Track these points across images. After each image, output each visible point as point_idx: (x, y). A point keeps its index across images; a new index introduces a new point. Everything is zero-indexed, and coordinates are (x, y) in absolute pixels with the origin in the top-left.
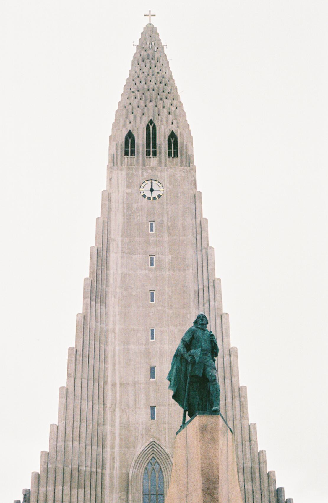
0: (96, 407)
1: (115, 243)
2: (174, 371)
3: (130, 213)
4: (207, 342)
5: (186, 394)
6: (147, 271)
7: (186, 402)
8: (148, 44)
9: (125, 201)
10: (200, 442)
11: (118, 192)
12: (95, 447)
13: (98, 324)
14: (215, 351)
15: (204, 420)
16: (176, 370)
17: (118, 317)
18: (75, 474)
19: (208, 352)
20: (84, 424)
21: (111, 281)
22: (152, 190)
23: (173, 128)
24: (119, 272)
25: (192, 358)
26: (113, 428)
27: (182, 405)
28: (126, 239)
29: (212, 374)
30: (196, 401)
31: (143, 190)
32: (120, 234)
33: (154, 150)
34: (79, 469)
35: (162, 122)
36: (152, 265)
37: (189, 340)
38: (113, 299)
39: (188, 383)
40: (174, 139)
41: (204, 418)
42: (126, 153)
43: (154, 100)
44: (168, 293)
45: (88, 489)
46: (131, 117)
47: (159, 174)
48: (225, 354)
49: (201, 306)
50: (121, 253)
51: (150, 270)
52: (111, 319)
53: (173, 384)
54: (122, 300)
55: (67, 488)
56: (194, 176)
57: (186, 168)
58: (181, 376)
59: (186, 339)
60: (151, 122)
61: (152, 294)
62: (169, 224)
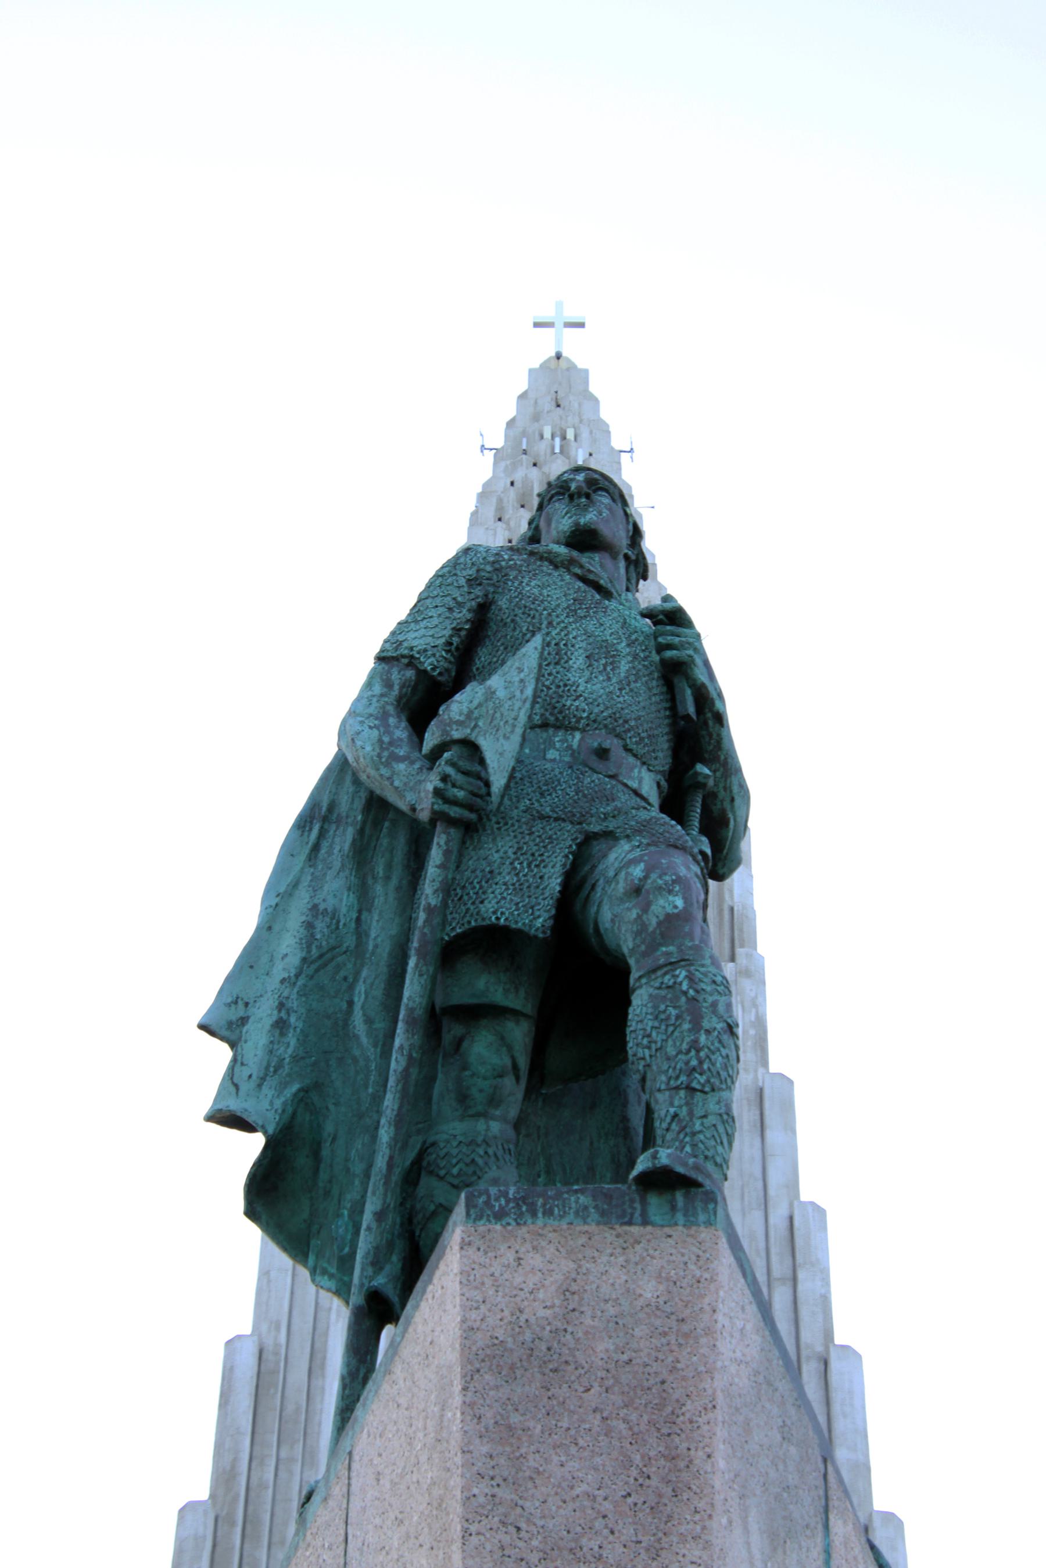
4: (624, 666)
7: (379, 1216)
8: (547, 435)
10: (466, 1534)
14: (702, 769)
15: (533, 1280)
16: (309, 939)
19: (627, 749)
39: (411, 1011)
41: (535, 1260)
56: (755, 1005)
58: (351, 1003)
59: (415, 643)
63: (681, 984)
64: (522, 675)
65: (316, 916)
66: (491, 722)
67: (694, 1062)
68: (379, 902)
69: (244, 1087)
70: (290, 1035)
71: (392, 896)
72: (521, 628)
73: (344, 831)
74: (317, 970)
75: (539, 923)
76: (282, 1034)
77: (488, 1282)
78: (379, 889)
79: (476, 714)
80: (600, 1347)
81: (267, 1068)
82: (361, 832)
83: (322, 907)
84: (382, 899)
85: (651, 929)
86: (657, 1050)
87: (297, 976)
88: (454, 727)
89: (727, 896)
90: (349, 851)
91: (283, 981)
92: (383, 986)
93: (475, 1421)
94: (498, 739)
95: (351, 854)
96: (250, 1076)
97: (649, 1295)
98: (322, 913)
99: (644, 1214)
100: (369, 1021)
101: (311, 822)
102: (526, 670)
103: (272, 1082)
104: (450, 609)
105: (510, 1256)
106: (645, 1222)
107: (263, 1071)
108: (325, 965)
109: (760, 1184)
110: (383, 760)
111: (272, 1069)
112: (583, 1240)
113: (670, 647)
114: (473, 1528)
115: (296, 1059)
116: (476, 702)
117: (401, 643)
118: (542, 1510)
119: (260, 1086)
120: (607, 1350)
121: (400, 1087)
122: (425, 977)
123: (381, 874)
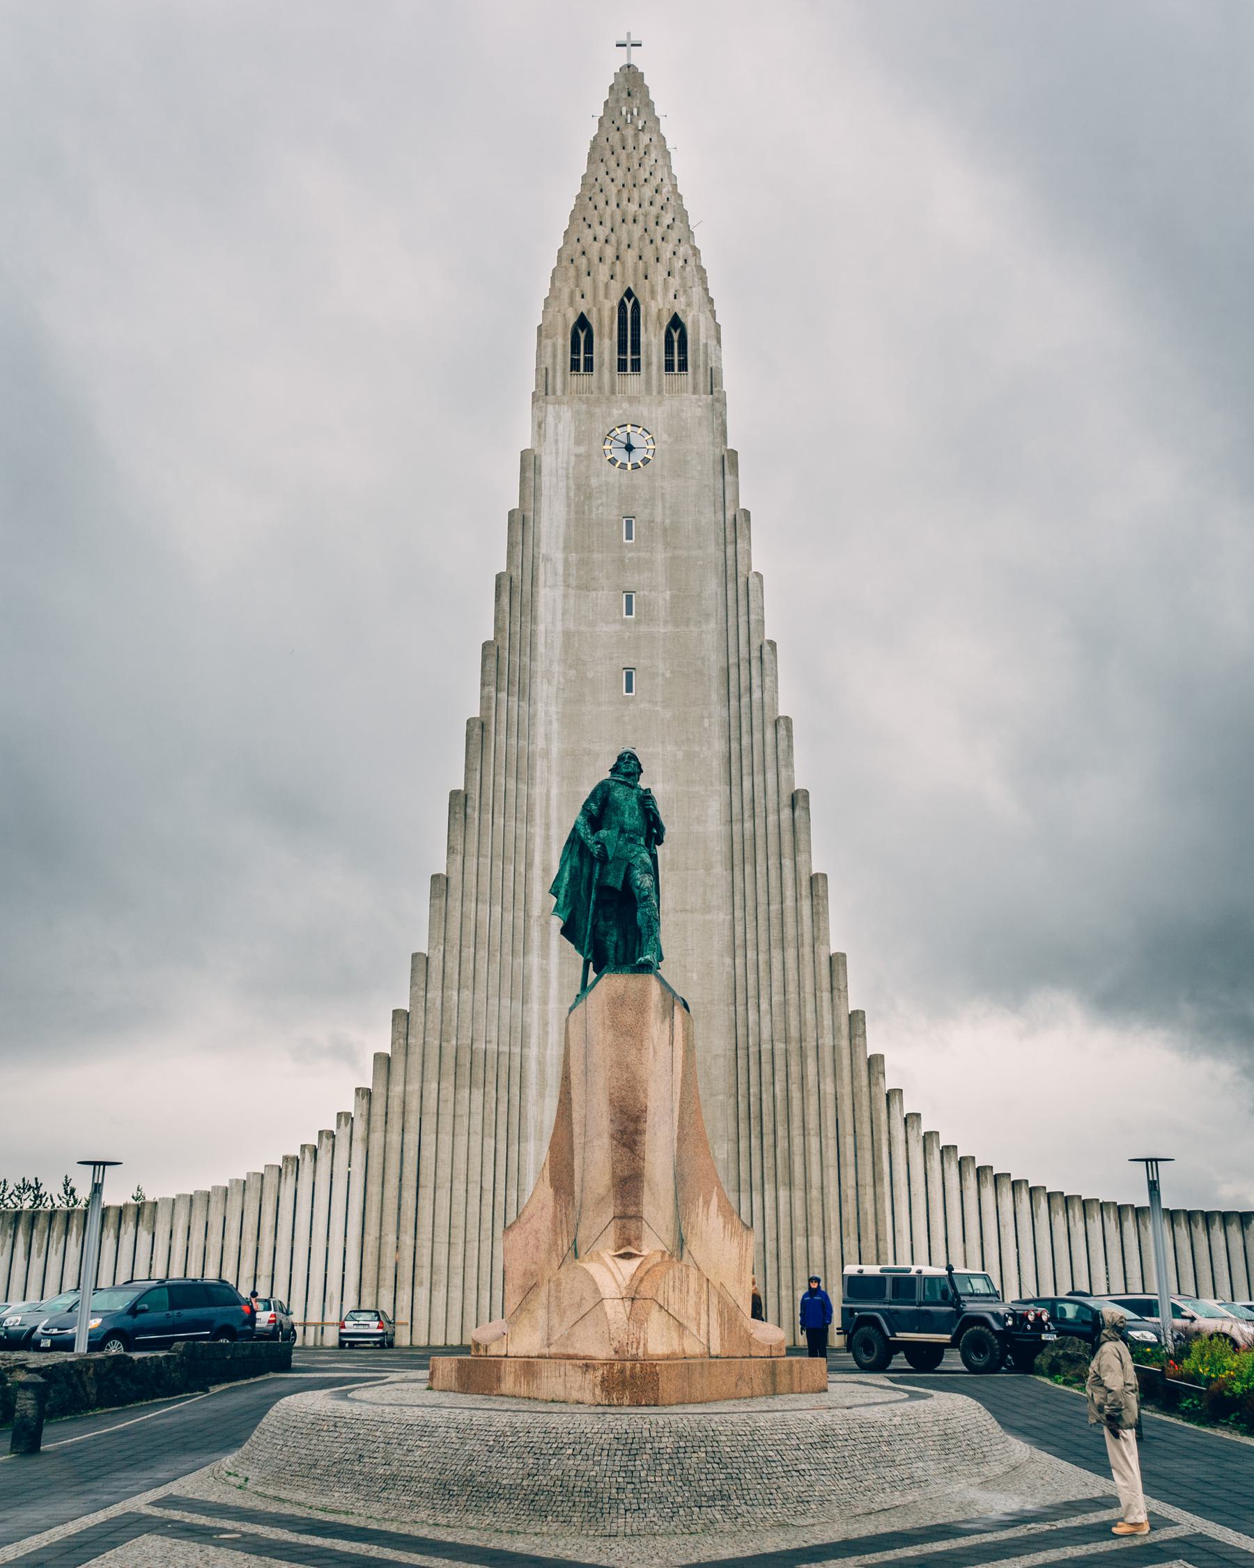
0: (509, 917)
1: (549, 565)
2: (566, 875)
3: (582, 498)
5: (589, 927)
6: (618, 627)
7: (589, 943)
8: (624, 113)
9: (571, 471)
11: (557, 453)
12: (506, 1002)
13: (513, 741)
17: (555, 726)
18: (465, 1059)
20: (483, 954)
21: (541, 649)
22: (629, 448)
23: (679, 306)
24: (559, 628)
25: (600, 848)
26: (545, 961)
27: (579, 948)
28: (573, 557)
29: (641, 883)
30: (611, 941)
31: (611, 447)
32: (561, 545)
33: (634, 357)
34: (474, 1048)
35: (653, 293)
36: (629, 612)
38: (545, 687)
40: (678, 331)
42: (575, 366)
43: (635, 244)
44: (663, 674)
45: (491, 1088)
46: (587, 282)
47: (646, 413)
48: (782, 805)
49: (733, 702)
50: (562, 588)
51: (624, 622)
52: (540, 730)
53: (561, 903)
54: (563, 689)
55: (448, 1084)
56: (721, 415)
57: (704, 396)
60: (629, 294)
61: (629, 676)
62: (667, 521)
89: (709, 362)
109: (722, 500)
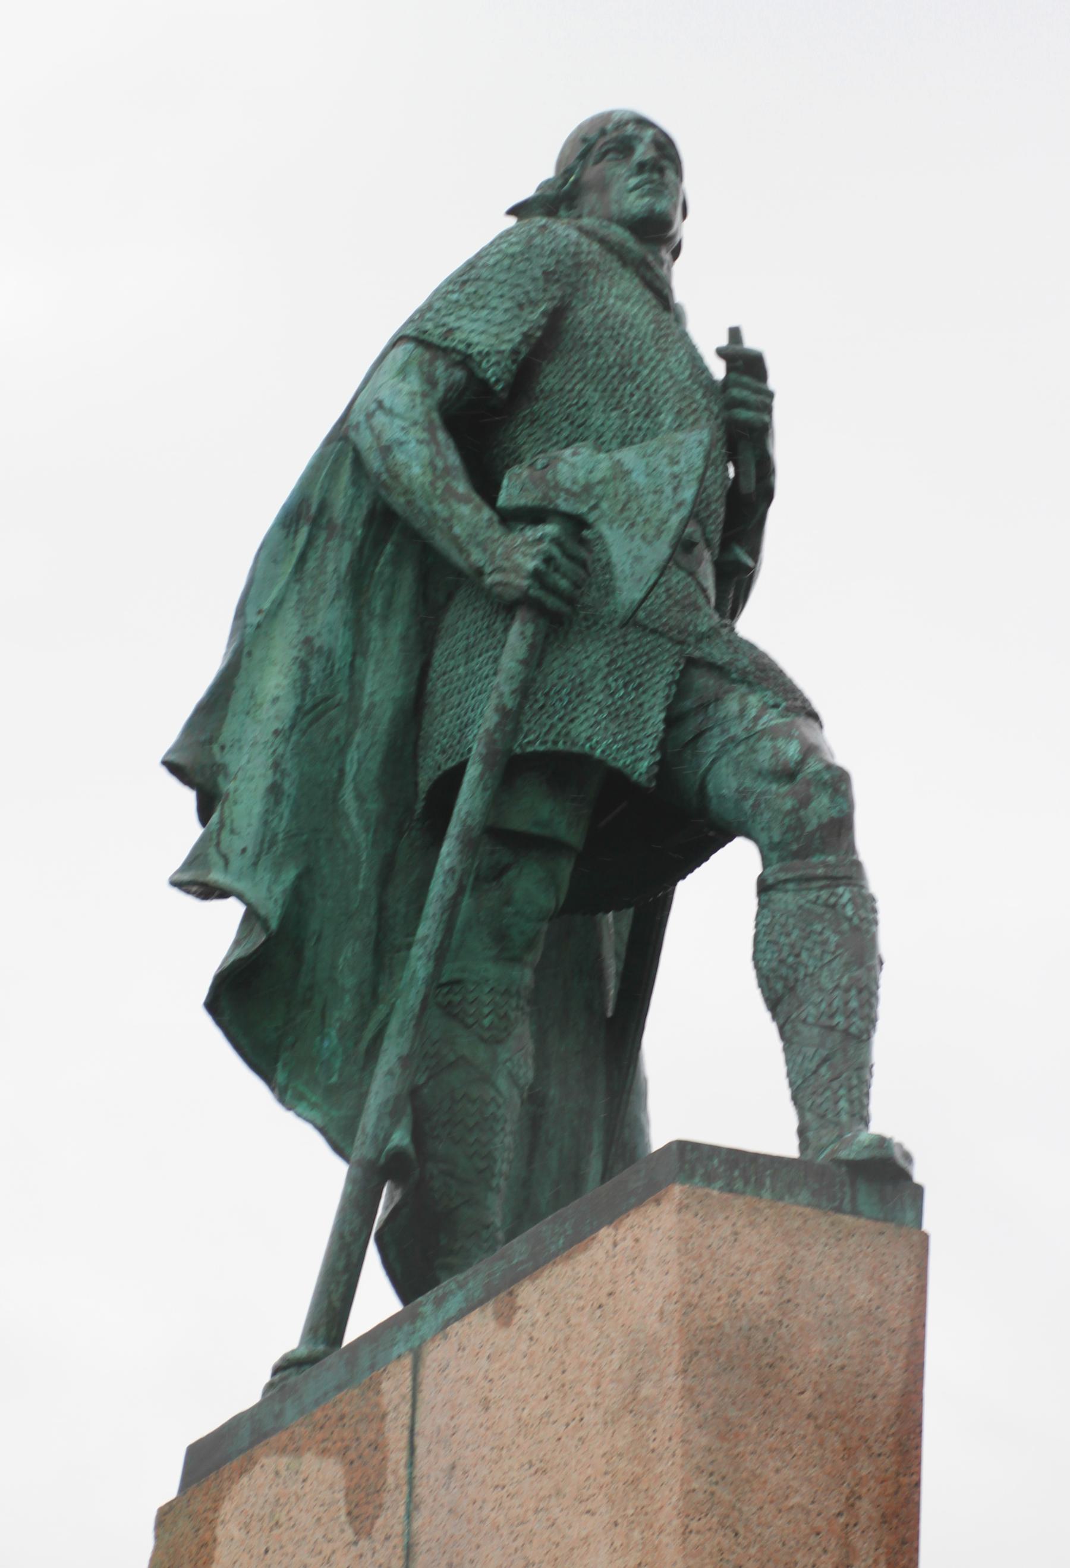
10: (686, 1531)
16: (303, 685)
25: (556, 541)
37: (506, 347)
39: (467, 830)
58: (342, 772)
59: (474, 338)
63: (844, 906)
64: (676, 469)
65: (310, 653)
66: (622, 510)
67: (854, 1004)
68: (375, 646)
69: (236, 863)
70: (284, 803)
71: (395, 648)
72: (607, 357)
73: (341, 545)
74: (310, 724)
75: (644, 765)
76: (277, 802)
77: (706, 1255)
78: (375, 629)
79: (598, 490)
80: (816, 1346)
81: (262, 842)
82: (359, 551)
83: (317, 643)
84: (379, 644)
85: (809, 829)
86: (806, 975)
87: (292, 727)
88: (563, 495)
90: (346, 575)
91: (276, 733)
92: (379, 758)
93: (694, 1408)
94: (632, 538)
95: (348, 578)
96: (244, 851)
97: (862, 1297)
98: (317, 652)
99: (853, 1200)
100: (360, 798)
101: (298, 521)
102: (682, 464)
103: (266, 861)
104: (521, 306)
105: (726, 1230)
106: (855, 1212)
107: (258, 848)
108: (317, 719)
110: (439, 492)
111: (266, 845)
112: (798, 1223)
113: (743, 404)
114: (694, 1525)
115: (290, 836)
116: (597, 476)
117: (451, 331)
118: (759, 1517)
119: (255, 864)
120: (821, 1352)
121: (445, 916)
122: (488, 793)
123: (378, 610)
